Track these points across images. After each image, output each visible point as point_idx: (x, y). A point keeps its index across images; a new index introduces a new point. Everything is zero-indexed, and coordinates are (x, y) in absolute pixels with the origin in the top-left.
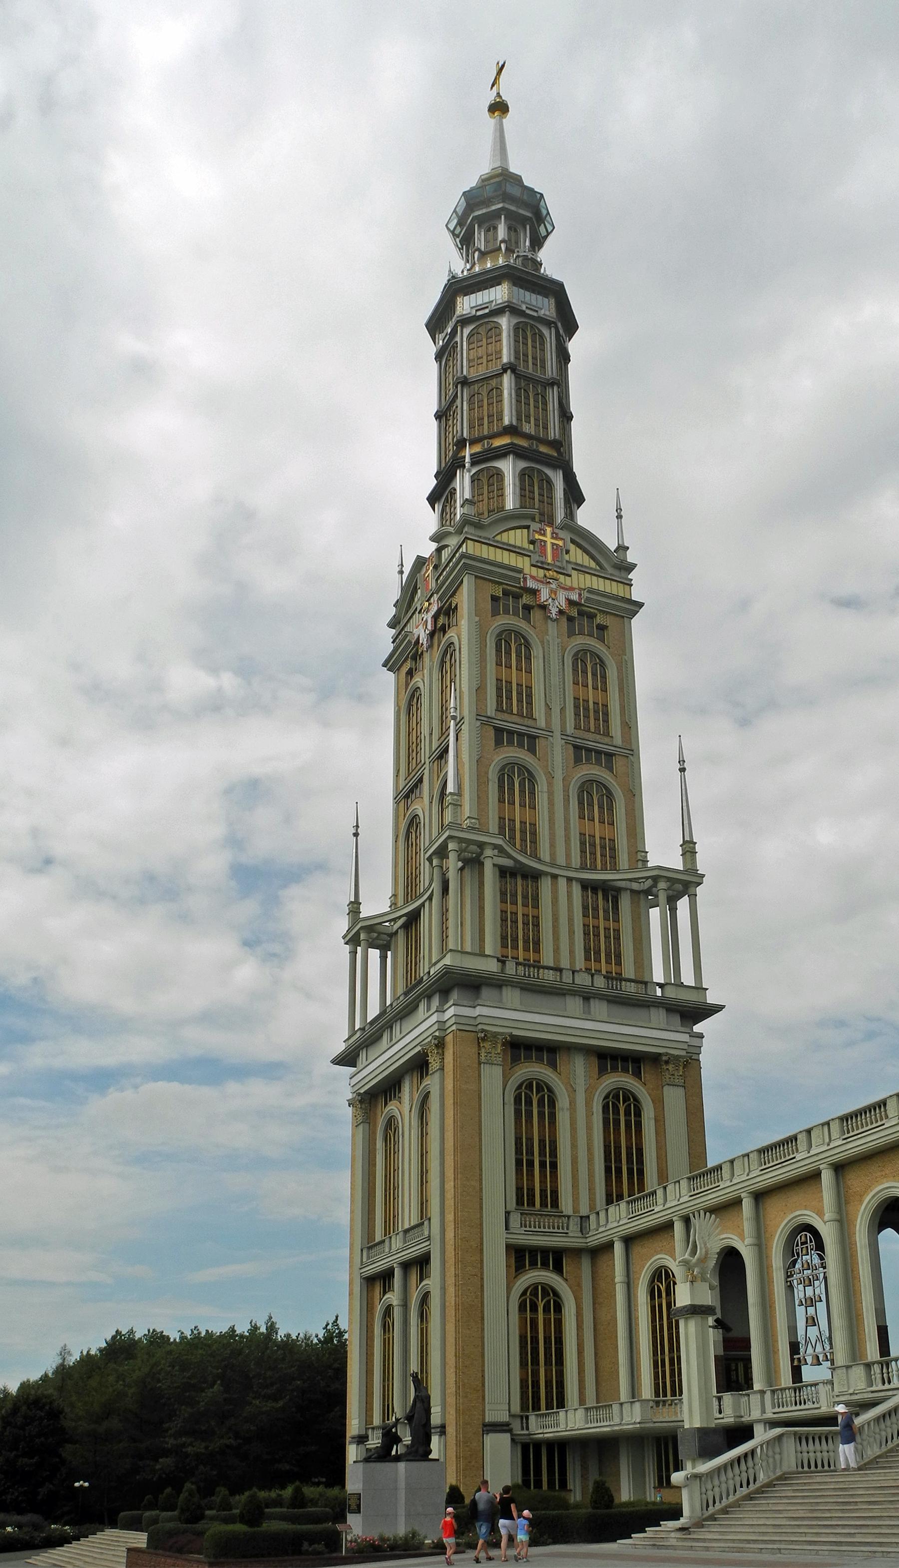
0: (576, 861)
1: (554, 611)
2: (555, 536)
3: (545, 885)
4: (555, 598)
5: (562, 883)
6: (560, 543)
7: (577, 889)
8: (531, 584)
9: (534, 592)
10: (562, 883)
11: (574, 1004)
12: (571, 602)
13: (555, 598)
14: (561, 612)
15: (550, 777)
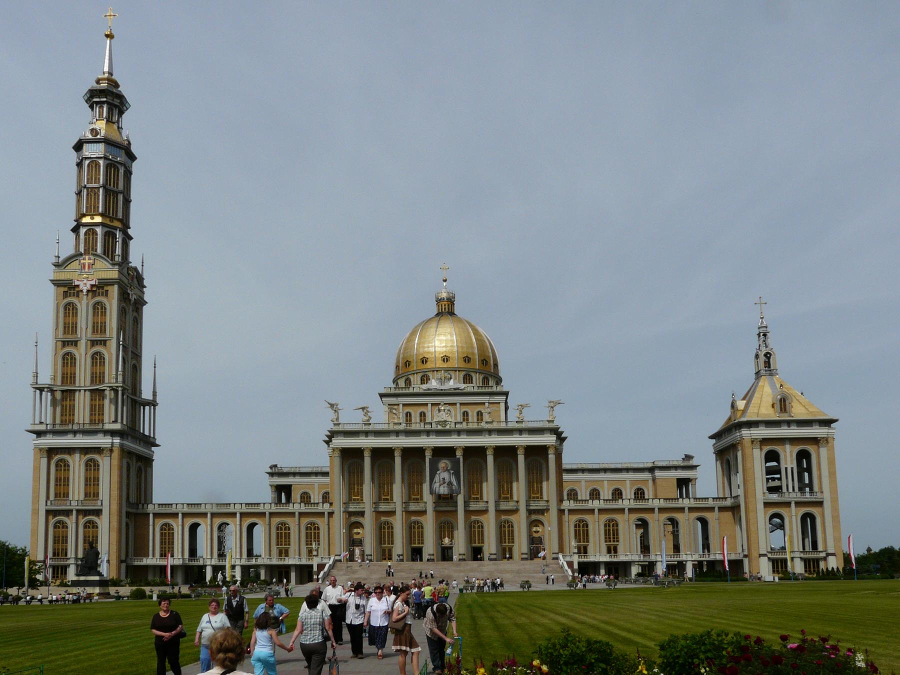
0: (88, 383)
1: (85, 291)
2: (90, 259)
3: (77, 394)
4: (85, 286)
5: (82, 392)
6: (91, 261)
7: (88, 393)
8: (77, 283)
9: (78, 286)
10: (82, 392)
11: (70, 436)
12: (92, 286)
13: (85, 286)
14: (88, 291)
15: (81, 355)
